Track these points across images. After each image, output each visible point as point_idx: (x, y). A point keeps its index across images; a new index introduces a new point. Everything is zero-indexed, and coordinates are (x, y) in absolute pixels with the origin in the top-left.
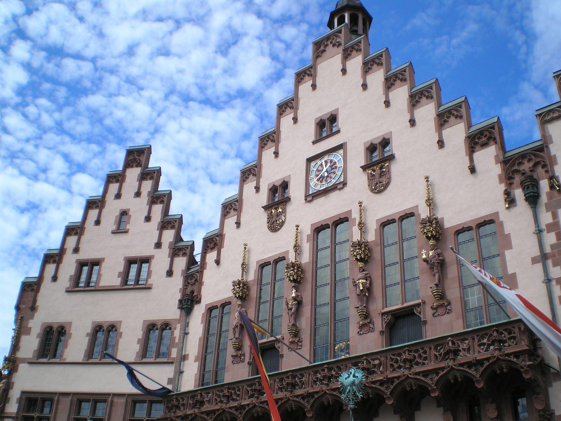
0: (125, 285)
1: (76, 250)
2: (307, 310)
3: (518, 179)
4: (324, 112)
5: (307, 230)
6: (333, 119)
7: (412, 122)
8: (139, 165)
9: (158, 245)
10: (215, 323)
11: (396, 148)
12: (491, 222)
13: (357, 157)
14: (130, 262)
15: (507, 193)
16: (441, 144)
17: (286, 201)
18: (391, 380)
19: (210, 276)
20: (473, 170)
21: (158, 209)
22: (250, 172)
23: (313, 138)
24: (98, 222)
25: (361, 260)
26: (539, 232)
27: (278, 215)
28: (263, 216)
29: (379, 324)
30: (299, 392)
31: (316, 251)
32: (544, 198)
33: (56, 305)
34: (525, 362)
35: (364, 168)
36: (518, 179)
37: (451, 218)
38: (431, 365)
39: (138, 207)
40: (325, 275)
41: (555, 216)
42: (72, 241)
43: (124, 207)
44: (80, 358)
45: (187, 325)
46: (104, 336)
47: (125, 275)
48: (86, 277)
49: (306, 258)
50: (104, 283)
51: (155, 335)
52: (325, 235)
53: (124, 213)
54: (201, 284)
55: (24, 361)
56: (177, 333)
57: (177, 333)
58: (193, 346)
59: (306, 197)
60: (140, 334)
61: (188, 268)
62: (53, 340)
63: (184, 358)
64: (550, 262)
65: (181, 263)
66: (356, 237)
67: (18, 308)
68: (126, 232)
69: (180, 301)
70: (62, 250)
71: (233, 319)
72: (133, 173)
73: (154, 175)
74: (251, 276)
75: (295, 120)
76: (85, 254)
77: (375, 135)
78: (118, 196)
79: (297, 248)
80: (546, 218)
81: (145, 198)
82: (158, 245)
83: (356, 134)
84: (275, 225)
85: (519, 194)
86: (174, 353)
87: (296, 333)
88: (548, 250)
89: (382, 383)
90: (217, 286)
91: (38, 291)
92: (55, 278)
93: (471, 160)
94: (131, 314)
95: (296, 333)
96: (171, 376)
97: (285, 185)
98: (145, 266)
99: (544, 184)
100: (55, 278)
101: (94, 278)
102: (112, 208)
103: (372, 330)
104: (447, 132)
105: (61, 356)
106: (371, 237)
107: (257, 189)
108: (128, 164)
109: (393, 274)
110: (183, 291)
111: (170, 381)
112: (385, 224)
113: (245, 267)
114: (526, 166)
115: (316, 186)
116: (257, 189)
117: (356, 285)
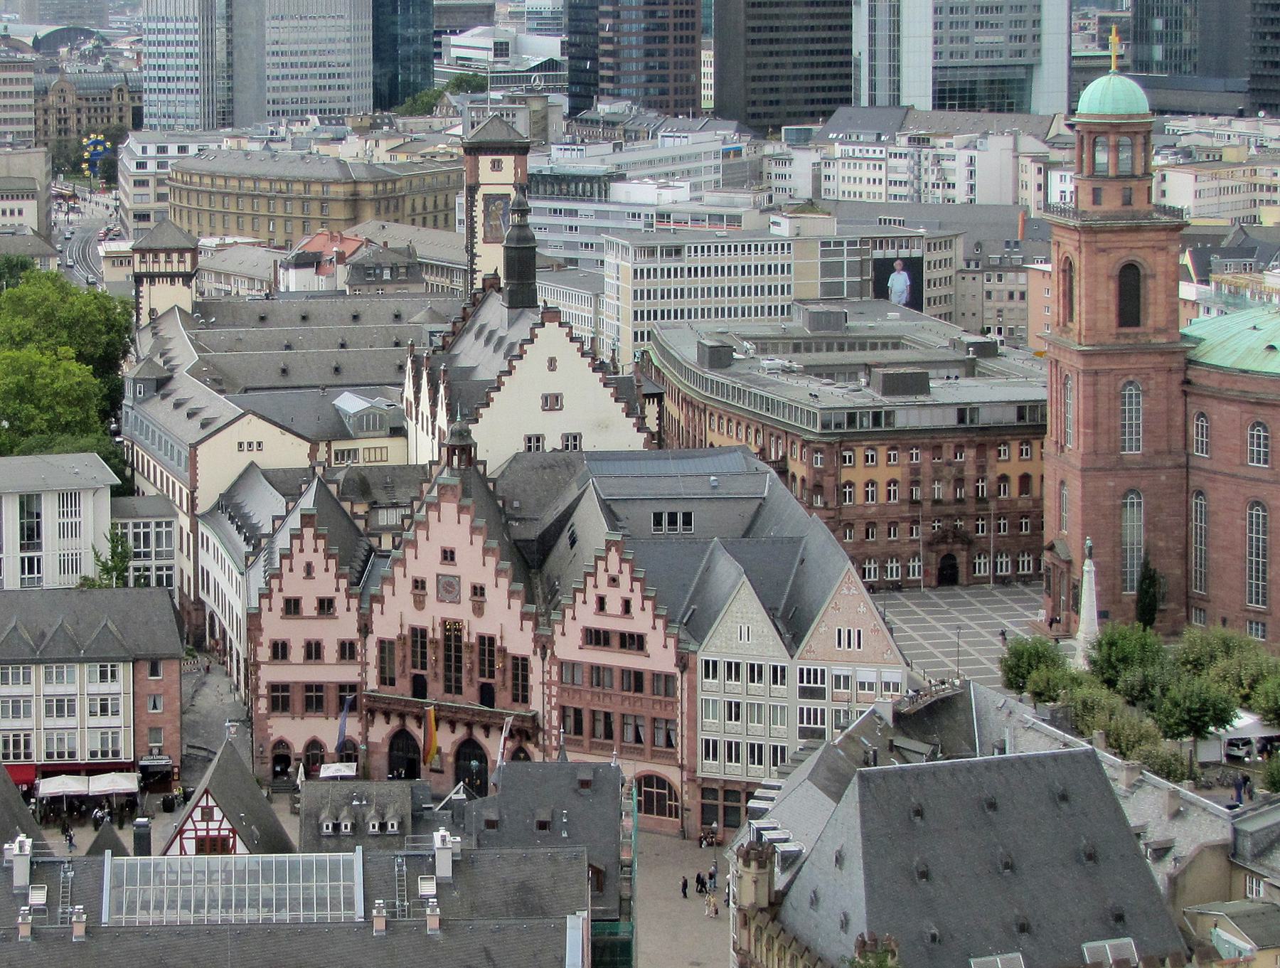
1: (280, 590)
5: (438, 620)
6: (452, 553)
9: (337, 590)
19: (376, 617)
24: (291, 570)
28: (410, 599)
29: (476, 686)
33: (275, 626)
39: (318, 560)
48: (292, 607)
49: (439, 635)
65: (354, 603)
70: (271, 590)
72: (309, 533)
74: (406, 632)
78: (301, 551)
80: (547, 668)
81: (321, 554)
82: (337, 590)
92: (270, 610)
97: (423, 583)
100: (270, 610)
106: (473, 640)
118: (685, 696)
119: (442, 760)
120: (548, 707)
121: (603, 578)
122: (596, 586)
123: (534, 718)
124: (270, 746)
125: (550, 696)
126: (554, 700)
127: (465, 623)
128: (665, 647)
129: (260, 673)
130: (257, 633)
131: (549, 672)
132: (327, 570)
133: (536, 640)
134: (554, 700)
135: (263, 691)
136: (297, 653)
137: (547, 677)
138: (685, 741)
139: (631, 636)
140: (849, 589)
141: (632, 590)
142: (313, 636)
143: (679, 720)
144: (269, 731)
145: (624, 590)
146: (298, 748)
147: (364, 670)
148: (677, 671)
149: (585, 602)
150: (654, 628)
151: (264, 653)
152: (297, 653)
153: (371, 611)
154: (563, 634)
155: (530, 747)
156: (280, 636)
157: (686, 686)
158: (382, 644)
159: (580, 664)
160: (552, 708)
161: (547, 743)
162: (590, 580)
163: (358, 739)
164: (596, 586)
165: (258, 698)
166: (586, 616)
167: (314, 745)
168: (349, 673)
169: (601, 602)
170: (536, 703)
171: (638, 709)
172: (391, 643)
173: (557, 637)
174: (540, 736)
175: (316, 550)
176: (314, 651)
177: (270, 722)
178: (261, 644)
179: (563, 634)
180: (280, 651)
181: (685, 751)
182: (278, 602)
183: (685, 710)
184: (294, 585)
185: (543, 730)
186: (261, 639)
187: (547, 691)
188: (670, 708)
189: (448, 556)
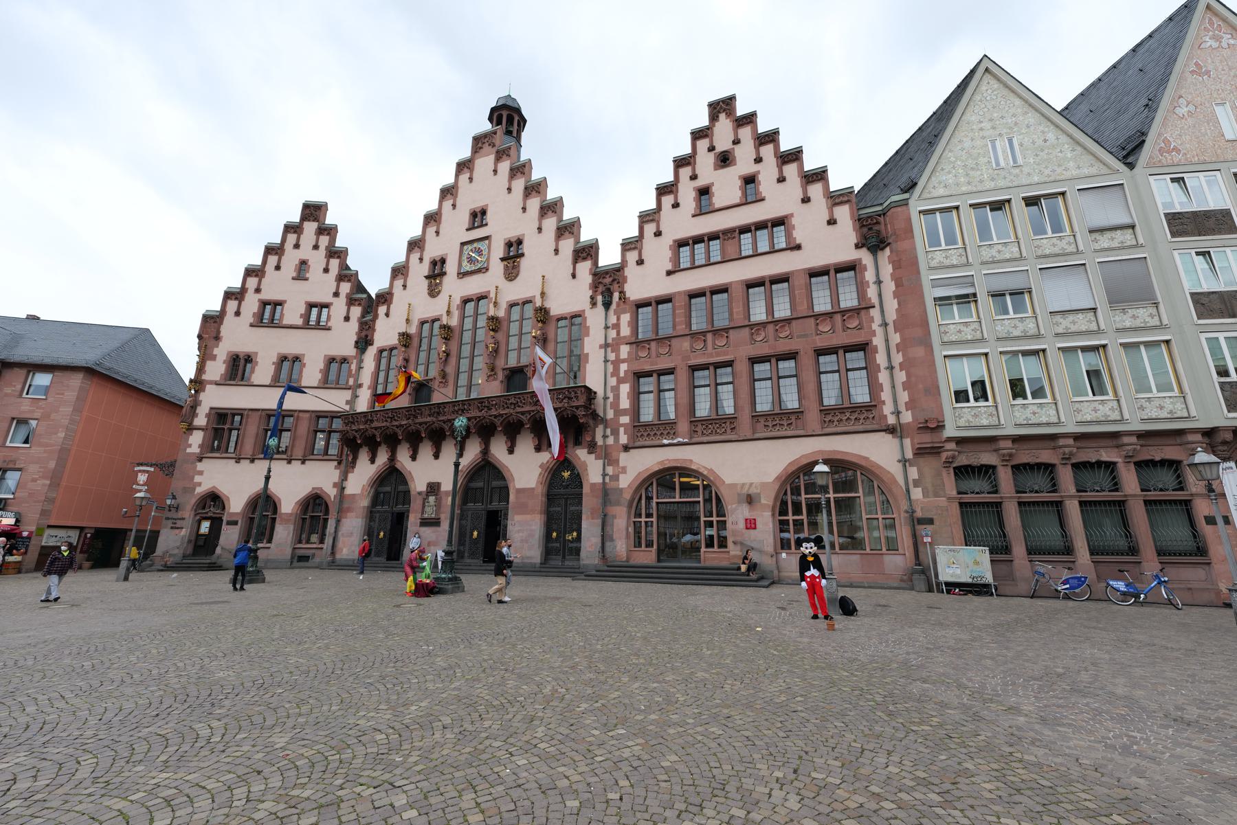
0: (306, 325)
1: (258, 290)
2: (453, 360)
3: (601, 288)
4: (477, 205)
5: (457, 301)
6: (484, 212)
7: (540, 229)
8: (316, 220)
9: (336, 294)
10: (384, 361)
11: (526, 248)
12: (580, 316)
13: (498, 251)
14: (311, 306)
15: (592, 298)
16: (557, 251)
17: (443, 274)
18: (501, 415)
20: (574, 276)
21: (335, 263)
22: (415, 245)
23: (467, 226)
24: (278, 268)
25: (493, 330)
26: (607, 328)
27: (436, 285)
29: (501, 376)
30: (441, 418)
31: (463, 317)
32: (614, 306)
33: (238, 335)
34: (581, 412)
35: (502, 259)
36: (601, 288)
37: (556, 309)
38: (527, 408)
39: (317, 260)
40: (467, 337)
41: (618, 319)
42: (252, 282)
43: (304, 257)
44: (268, 381)
45: (362, 361)
46: (289, 364)
47: (306, 317)
50: (286, 322)
51: (334, 366)
52: (470, 306)
53: (303, 263)
54: (374, 330)
55: (211, 382)
56: (353, 367)
57: (353, 367)
58: (366, 377)
59: (459, 274)
60: (322, 366)
61: (363, 316)
62: (239, 368)
63: (360, 386)
64: (609, 349)
65: (356, 311)
66: (491, 313)
67: (200, 337)
68: (307, 279)
69: (357, 342)
70: (243, 290)
71: (397, 360)
72: (310, 227)
73: (331, 231)
75: (454, 206)
76: (265, 295)
77: (512, 234)
78: (297, 246)
79: (448, 312)
81: (322, 251)
82: (336, 294)
83: (500, 229)
84: (433, 292)
85: (599, 298)
86: (351, 382)
87: (444, 375)
88: (610, 341)
89: (496, 417)
90: (386, 332)
91: (221, 323)
92: (238, 314)
93: (574, 269)
94: (314, 349)
95: (444, 375)
96: (349, 398)
97: (443, 261)
98: (325, 311)
99: (616, 295)
100: (238, 314)
101: (277, 316)
102: (291, 259)
103: (495, 379)
104: (562, 243)
105: (249, 379)
107: (421, 259)
108: (304, 218)
109: (514, 343)
110: (359, 334)
111: (348, 402)
112: (512, 305)
113: (408, 321)
114: (608, 280)
115: (467, 267)
116: (421, 259)
117: (487, 347)
118: (889, 286)
119: (438, 504)
120: (613, 381)
121: (705, 162)
122: (694, 177)
123: (590, 394)
124: (193, 501)
125: (617, 363)
126: (624, 367)
127: (492, 295)
128: (832, 222)
129: (202, 396)
130: (213, 342)
131: (617, 326)
132: (326, 270)
133: (595, 286)
134: (624, 367)
135: (201, 420)
136: (263, 371)
137: (612, 334)
138: (901, 376)
139: (761, 226)
140: (1218, 39)
141: (758, 160)
142: (291, 349)
143: (878, 341)
144: (197, 479)
145: (744, 162)
146: (236, 504)
147: (355, 396)
148: (865, 256)
149: (676, 205)
150: (806, 200)
151: (216, 369)
152: (263, 371)
153: (376, 316)
154: (640, 262)
155: (582, 454)
156: (242, 348)
157: (887, 270)
158: (381, 351)
159: (667, 300)
160: (620, 381)
161: (610, 441)
162: (685, 172)
163: (332, 492)
164: (694, 177)
165: (191, 428)
166: (682, 222)
167: (264, 504)
168: (336, 400)
169: (704, 192)
170: (594, 377)
171: (784, 346)
172: (392, 349)
173: (631, 271)
174: (599, 431)
175: (316, 247)
176: (288, 371)
177: (200, 466)
178: (214, 358)
179: (640, 262)
180: (239, 368)
181: (904, 397)
182: (251, 304)
183: (891, 316)
184: (276, 285)
185: (604, 421)
186: (216, 351)
187: (612, 356)
188: (854, 323)
189: (478, 217)
